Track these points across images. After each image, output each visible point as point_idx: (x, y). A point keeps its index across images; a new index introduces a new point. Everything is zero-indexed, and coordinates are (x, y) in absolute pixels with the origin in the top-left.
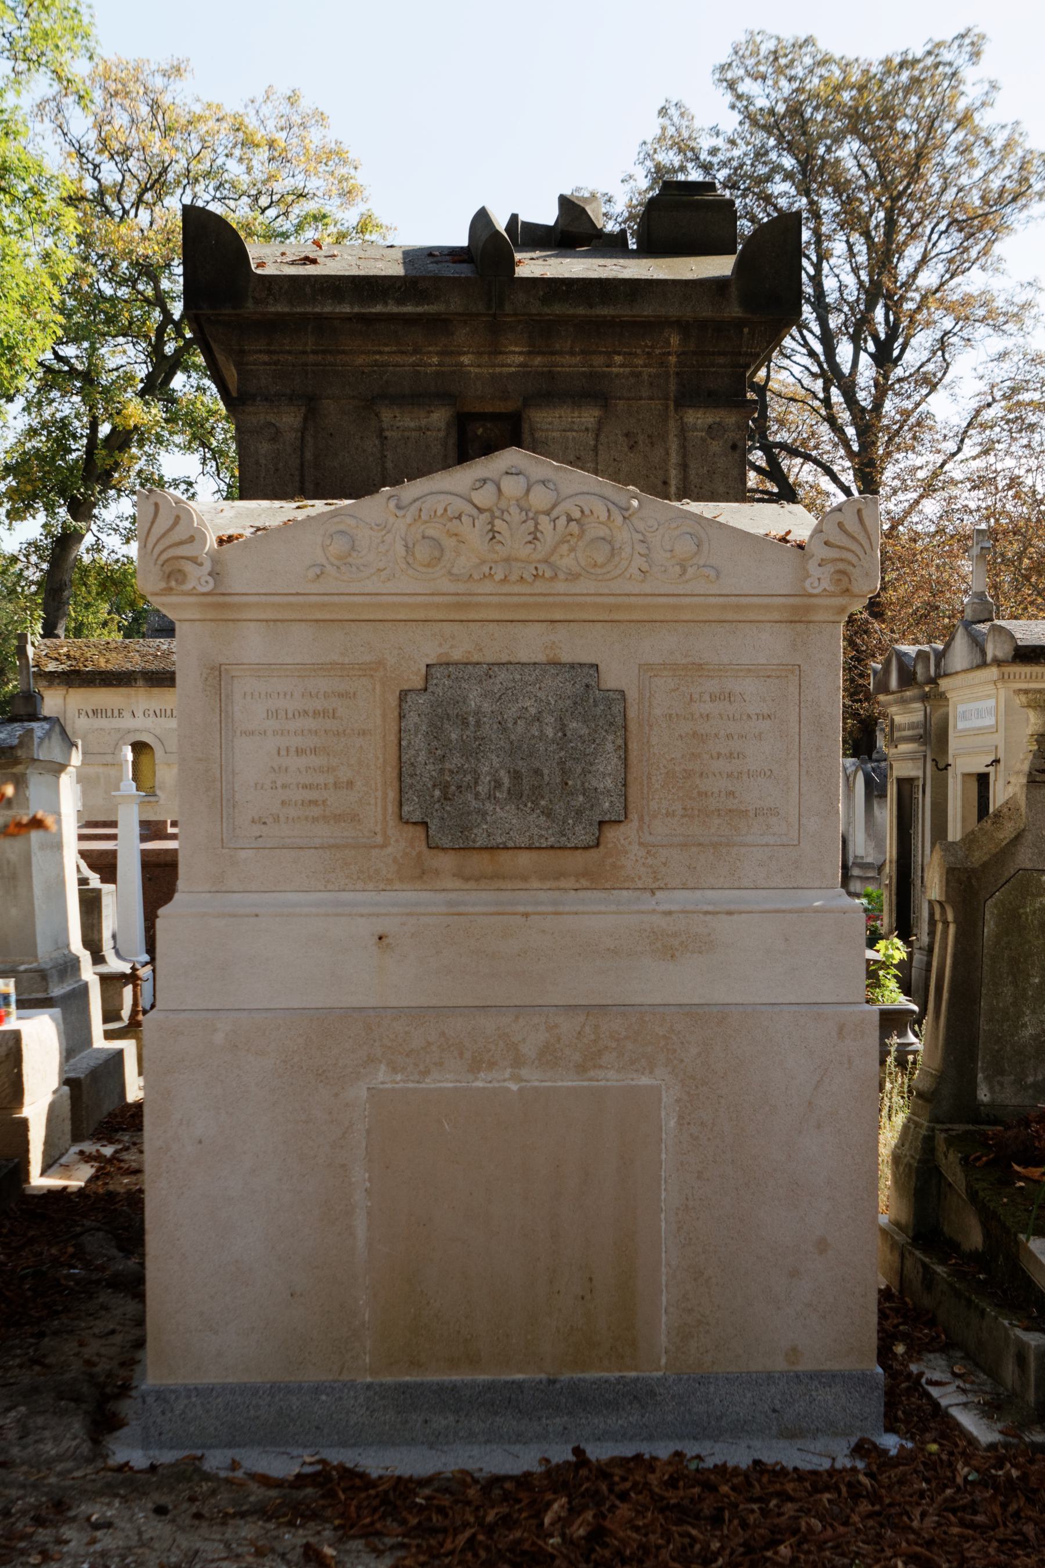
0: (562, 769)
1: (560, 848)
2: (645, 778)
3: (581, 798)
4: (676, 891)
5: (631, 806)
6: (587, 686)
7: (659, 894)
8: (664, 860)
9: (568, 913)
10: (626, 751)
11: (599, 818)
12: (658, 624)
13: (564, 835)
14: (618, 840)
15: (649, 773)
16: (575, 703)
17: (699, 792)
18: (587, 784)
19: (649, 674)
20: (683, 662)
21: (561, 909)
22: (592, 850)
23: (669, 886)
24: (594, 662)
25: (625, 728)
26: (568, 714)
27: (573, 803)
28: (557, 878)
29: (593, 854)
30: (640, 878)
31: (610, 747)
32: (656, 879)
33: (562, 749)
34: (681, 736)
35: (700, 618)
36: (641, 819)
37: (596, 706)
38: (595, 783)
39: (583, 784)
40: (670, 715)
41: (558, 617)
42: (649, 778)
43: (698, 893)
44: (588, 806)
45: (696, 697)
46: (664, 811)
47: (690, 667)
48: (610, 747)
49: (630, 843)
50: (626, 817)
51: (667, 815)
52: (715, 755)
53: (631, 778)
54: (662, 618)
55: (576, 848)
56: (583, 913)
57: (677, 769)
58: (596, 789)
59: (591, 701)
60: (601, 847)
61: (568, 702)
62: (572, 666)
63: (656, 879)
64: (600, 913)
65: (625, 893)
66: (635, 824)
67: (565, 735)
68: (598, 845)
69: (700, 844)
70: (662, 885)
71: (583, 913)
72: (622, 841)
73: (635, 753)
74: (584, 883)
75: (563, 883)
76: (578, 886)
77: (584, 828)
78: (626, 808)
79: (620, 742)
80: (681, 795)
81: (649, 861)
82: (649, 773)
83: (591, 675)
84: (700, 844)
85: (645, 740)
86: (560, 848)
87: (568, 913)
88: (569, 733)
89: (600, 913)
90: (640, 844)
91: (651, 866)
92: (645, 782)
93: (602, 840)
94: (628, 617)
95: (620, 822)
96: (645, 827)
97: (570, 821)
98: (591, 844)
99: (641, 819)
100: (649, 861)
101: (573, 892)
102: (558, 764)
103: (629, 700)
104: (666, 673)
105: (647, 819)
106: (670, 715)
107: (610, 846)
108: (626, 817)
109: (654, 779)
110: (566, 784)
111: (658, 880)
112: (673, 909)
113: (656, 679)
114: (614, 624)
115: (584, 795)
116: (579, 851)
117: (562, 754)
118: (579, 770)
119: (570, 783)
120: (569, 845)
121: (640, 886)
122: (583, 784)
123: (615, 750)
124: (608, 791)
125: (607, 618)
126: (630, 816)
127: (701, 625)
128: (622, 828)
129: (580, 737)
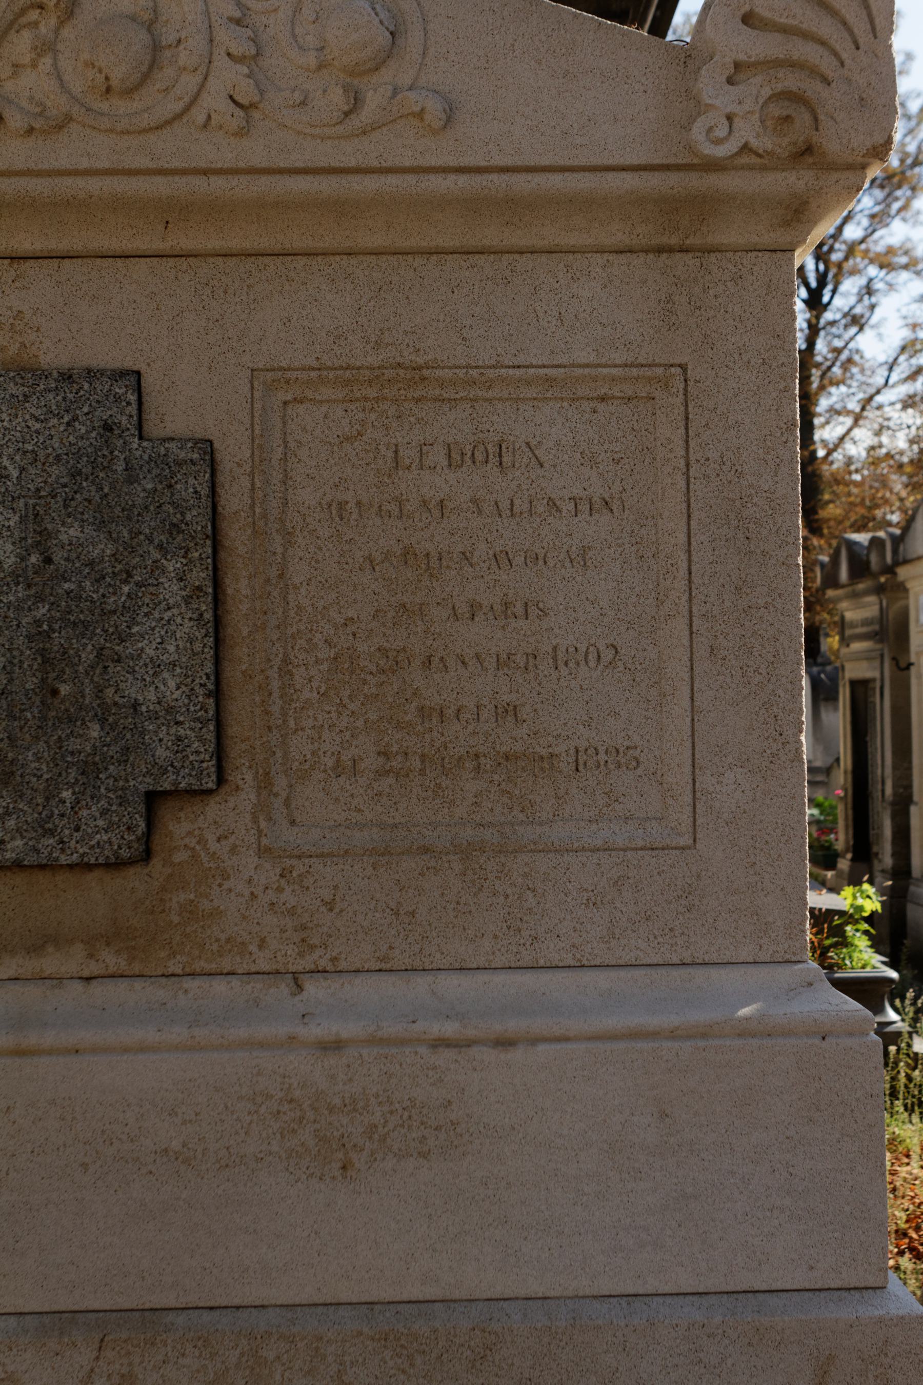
0: (42, 652)
1: (42, 867)
2: (273, 673)
3: (95, 731)
4: (359, 980)
5: (236, 751)
6: (107, 427)
7: (314, 989)
8: (327, 894)
9: (50, 1052)
10: (218, 600)
11: (145, 784)
12: (302, 261)
13: (51, 832)
14: (202, 841)
15: (286, 661)
16: (75, 474)
17: (421, 709)
18: (110, 692)
19: (282, 396)
20: (372, 360)
21: (32, 1039)
22: (132, 871)
23: (343, 965)
24: (128, 364)
25: (216, 539)
26: (56, 504)
27: (73, 744)
28: (35, 949)
29: (134, 878)
30: (262, 944)
31: (171, 591)
32: (306, 947)
33: (40, 598)
34: (370, 559)
35: (412, 242)
36: (265, 783)
37: (131, 480)
38: (133, 691)
39: (99, 691)
40: (342, 505)
41: (26, 243)
42: (286, 670)
43: (422, 982)
44: (113, 751)
45: (408, 454)
46: (330, 762)
47: (389, 373)
48: (171, 591)
49: (233, 850)
50: (221, 780)
51: (338, 770)
52: (463, 609)
53: (233, 673)
54: (308, 243)
55: (85, 867)
56: (95, 1050)
57: (362, 647)
58: (135, 706)
59: (120, 466)
60: (156, 862)
61: (55, 471)
62: (67, 377)
63: (306, 947)
64: (142, 1049)
65: (219, 986)
66: (247, 797)
67: (48, 560)
68: (147, 855)
69: (426, 850)
70: (323, 963)
71: (95, 1050)
72: (213, 846)
73: (244, 607)
74: (111, 960)
75: (50, 963)
76: (93, 968)
77: (104, 812)
78: (220, 755)
79: (200, 576)
80: (373, 716)
81: (288, 897)
82: (286, 661)
83: (117, 399)
84: (426, 850)
85: (273, 572)
86: (42, 867)
87: (50, 1052)
88: (58, 556)
89: (142, 1049)
90: (263, 852)
91: (292, 912)
92: (275, 684)
93: (158, 840)
94: (215, 243)
95: (210, 792)
96: (278, 803)
97: (66, 794)
98: (125, 853)
99: (265, 783)
100: (288, 897)
101: (78, 986)
102: (30, 638)
103: (226, 464)
104: (326, 392)
105: (280, 783)
106: (342, 505)
107: (180, 856)
108: (221, 780)
109: (299, 674)
110: (55, 692)
111: (312, 947)
112: (344, 1035)
113: (301, 409)
114: (183, 263)
115: (103, 721)
116: (97, 873)
117: (43, 610)
118: (88, 655)
119: (64, 689)
120: (63, 859)
121: (266, 967)
122: (99, 691)
123: (187, 600)
124: (170, 710)
125: (158, 246)
126: (234, 777)
127: (419, 261)
128: (213, 808)
129: (91, 564)
